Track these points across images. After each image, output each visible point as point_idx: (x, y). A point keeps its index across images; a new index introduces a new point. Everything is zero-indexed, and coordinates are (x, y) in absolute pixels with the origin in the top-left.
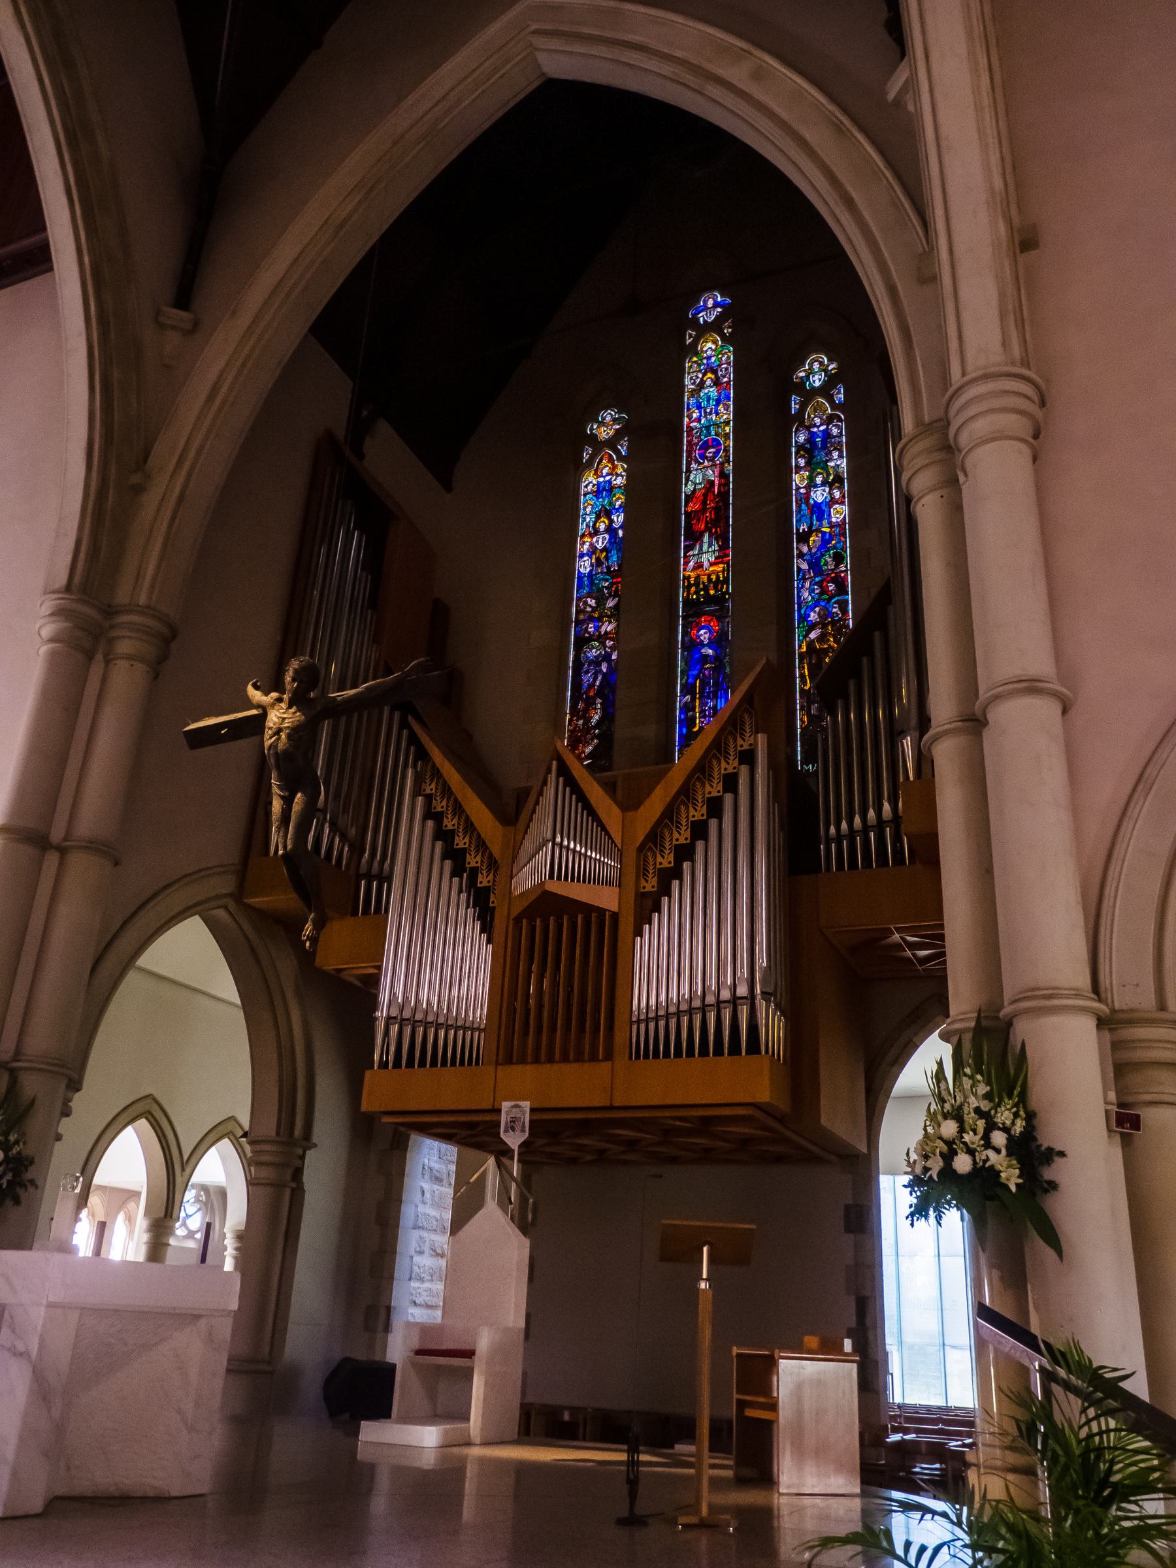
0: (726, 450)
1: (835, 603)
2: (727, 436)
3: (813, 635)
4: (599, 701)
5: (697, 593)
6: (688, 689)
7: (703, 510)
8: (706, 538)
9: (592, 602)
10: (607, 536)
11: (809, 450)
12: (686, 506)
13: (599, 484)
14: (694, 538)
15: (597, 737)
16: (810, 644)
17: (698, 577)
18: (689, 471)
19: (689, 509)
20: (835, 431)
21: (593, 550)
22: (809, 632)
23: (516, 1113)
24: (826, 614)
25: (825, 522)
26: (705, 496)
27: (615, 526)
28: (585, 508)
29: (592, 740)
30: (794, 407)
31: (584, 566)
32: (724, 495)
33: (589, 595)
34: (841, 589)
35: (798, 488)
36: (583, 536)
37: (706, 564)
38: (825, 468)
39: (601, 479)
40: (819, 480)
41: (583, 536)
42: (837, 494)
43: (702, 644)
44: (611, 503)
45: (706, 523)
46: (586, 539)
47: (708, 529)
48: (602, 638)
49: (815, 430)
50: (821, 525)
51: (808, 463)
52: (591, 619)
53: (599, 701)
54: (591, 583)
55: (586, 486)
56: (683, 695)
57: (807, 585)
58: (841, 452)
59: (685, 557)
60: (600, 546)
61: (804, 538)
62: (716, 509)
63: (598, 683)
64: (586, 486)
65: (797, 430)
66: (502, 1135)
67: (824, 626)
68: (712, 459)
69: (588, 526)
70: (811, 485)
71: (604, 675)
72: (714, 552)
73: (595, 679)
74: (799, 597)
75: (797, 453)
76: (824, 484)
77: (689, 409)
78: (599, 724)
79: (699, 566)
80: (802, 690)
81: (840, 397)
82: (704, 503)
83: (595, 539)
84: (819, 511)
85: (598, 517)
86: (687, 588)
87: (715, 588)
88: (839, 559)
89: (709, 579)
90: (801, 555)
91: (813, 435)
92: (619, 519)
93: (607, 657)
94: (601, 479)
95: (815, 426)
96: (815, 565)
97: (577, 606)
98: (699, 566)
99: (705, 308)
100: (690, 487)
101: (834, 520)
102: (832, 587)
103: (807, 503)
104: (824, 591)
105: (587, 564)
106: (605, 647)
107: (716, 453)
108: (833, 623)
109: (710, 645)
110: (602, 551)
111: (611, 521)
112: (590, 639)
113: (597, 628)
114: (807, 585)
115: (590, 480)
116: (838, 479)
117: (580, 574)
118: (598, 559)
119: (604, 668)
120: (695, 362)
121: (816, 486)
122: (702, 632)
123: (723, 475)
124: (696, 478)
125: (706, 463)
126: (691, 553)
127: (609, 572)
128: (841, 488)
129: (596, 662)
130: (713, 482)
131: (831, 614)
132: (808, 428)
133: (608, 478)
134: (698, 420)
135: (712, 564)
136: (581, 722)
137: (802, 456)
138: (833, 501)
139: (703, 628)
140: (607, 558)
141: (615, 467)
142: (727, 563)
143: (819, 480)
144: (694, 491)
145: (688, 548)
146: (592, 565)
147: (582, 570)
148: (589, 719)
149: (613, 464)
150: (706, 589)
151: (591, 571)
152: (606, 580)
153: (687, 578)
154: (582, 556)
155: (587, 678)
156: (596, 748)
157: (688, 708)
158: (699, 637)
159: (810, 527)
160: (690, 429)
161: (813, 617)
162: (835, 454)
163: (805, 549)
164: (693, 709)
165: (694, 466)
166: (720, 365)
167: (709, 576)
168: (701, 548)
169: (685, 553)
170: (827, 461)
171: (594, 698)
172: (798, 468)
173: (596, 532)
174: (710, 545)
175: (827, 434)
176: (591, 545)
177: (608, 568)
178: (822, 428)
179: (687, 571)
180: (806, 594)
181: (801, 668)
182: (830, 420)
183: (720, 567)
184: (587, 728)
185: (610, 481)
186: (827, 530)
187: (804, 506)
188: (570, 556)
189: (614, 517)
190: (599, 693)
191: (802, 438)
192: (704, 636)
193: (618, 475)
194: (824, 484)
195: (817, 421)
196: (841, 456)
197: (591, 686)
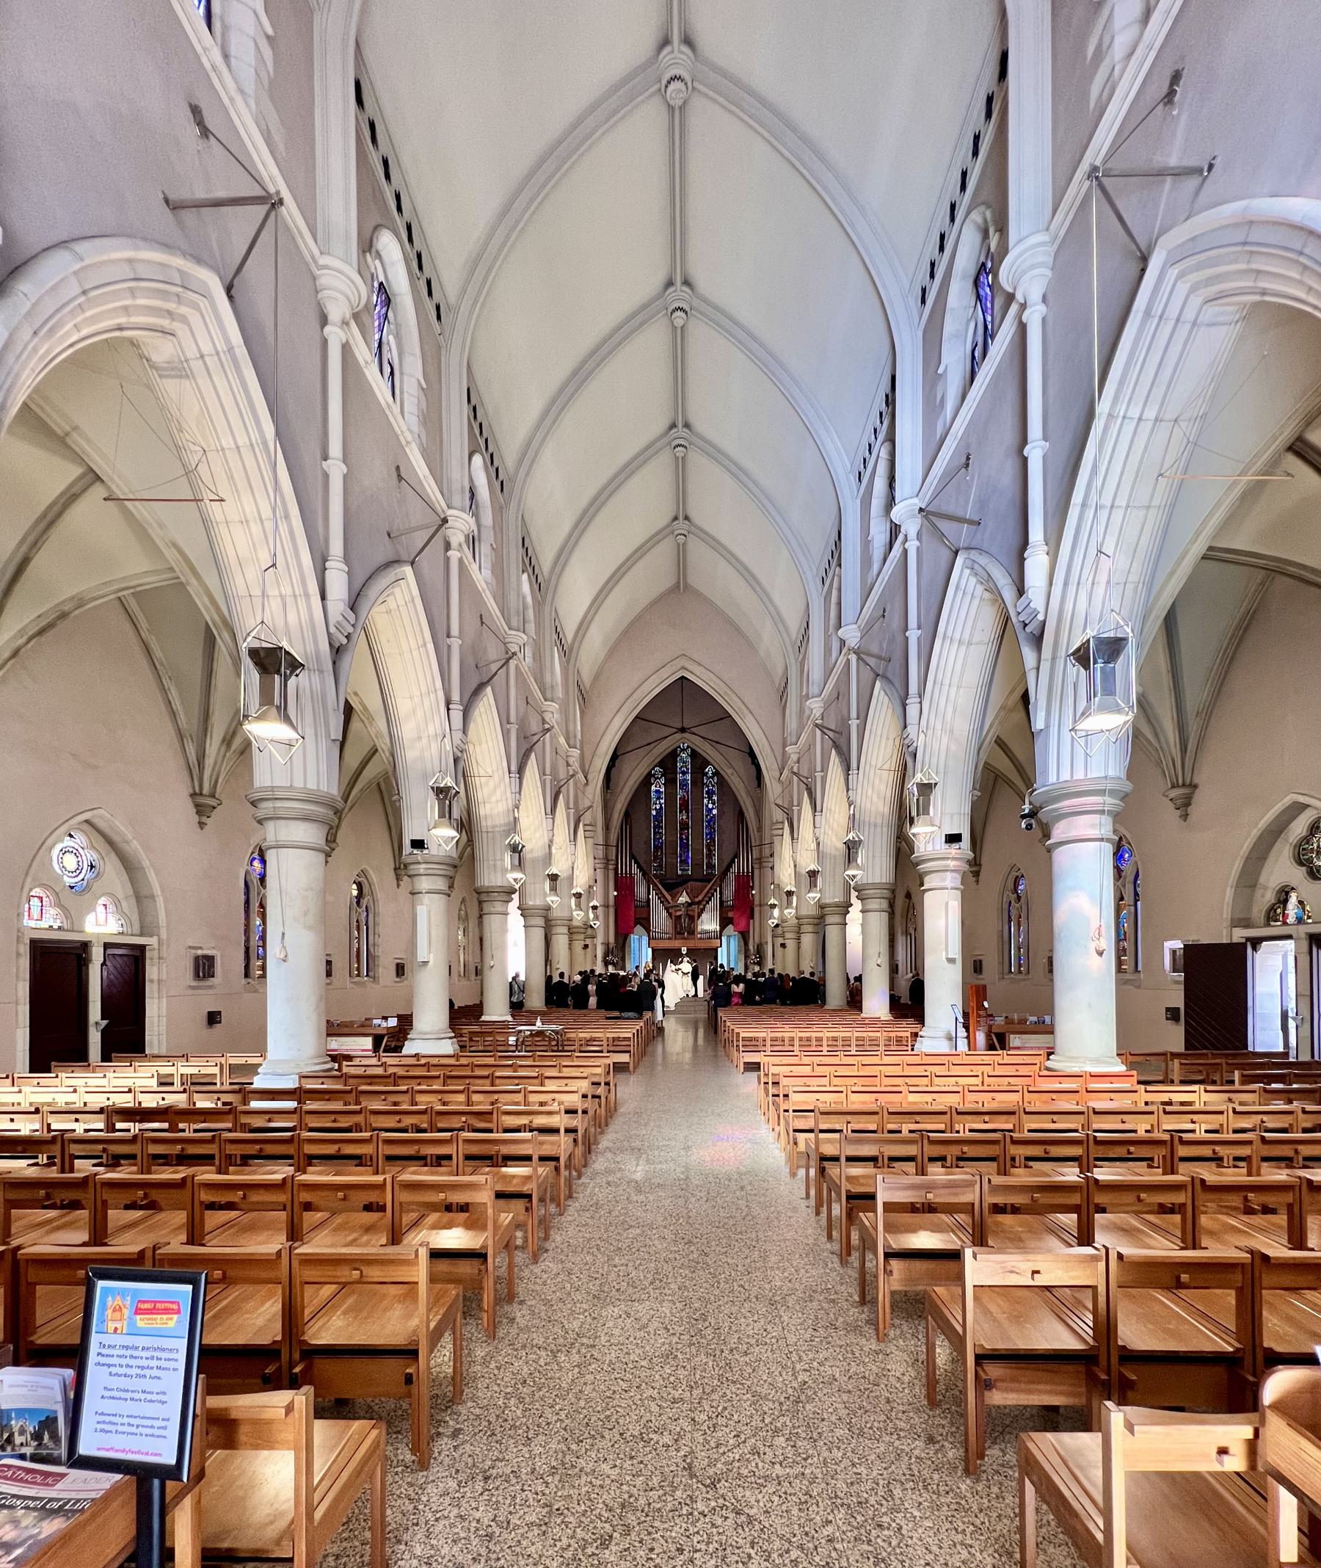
11: (707, 792)
92: (662, 801)
96: (708, 822)
115: (653, 788)
188: (650, 809)
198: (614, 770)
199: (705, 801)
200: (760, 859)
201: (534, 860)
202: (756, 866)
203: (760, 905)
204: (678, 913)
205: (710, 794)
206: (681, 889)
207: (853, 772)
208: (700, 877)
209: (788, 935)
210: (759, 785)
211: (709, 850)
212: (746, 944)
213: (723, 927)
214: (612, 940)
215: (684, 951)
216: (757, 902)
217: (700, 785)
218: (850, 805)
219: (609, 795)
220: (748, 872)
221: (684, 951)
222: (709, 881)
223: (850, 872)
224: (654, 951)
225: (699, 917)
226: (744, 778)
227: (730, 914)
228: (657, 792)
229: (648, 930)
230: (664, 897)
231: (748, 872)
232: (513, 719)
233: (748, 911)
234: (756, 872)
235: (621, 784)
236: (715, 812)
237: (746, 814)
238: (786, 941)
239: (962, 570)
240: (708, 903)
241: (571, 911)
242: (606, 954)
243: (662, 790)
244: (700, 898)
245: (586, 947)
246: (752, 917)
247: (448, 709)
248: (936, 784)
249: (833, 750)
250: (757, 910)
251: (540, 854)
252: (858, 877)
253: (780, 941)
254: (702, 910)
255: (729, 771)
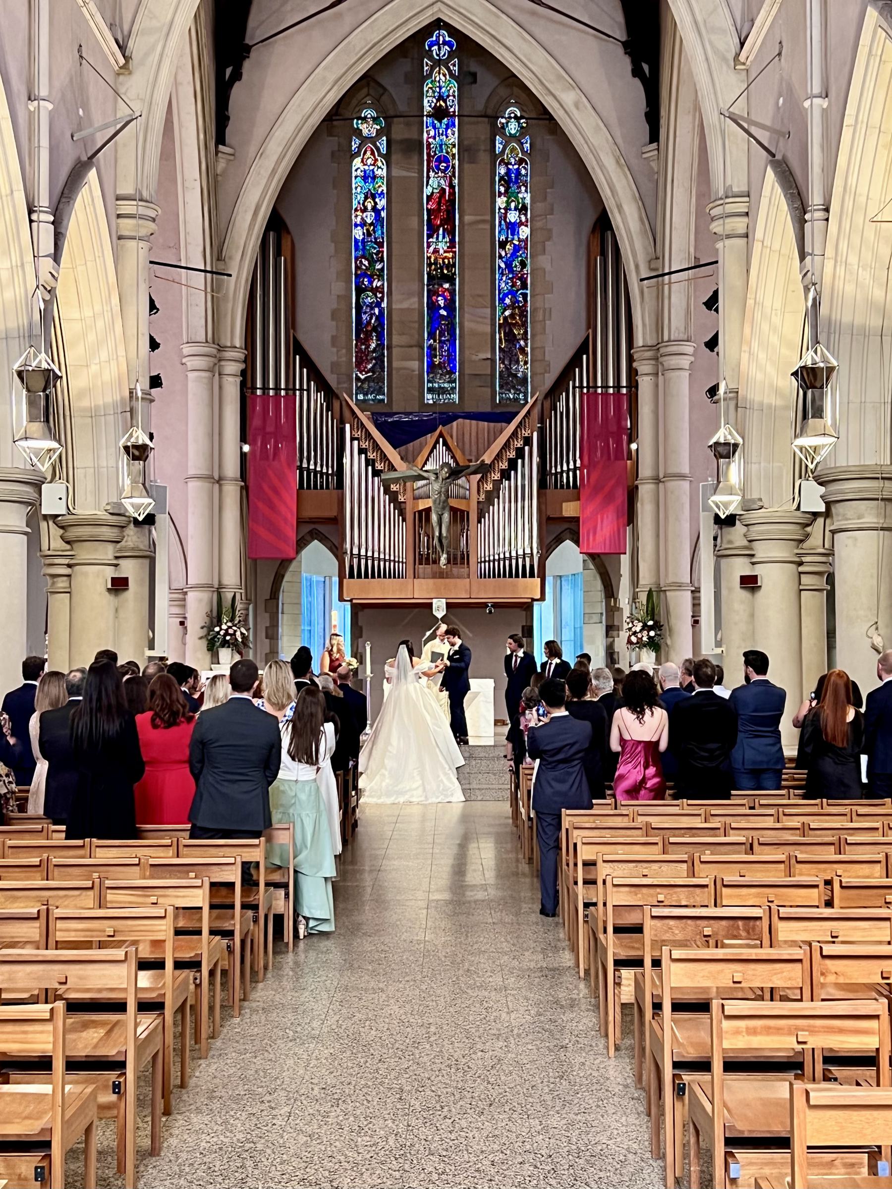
0: (453, 167)
1: (521, 294)
2: (454, 155)
3: (507, 313)
4: (374, 334)
5: (435, 270)
6: (431, 335)
7: (438, 210)
8: (441, 232)
9: (366, 263)
10: (373, 214)
11: (507, 181)
12: (427, 204)
13: (365, 171)
14: (433, 230)
15: (375, 358)
16: (505, 318)
17: (436, 259)
18: (428, 177)
19: (429, 207)
20: (523, 172)
21: (363, 224)
22: (505, 310)
23: (439, 604)
24: (515, 302)
25: (516, 237)
26: (440, 198)
27: (379, 207)
28: (356, 188)
29: (371, 359)
30: (499, 147)
31: (358, 233)
32: (452, 201)
33: (363, 257)
34: (524, 286)
35: (500, 209)
36: (356, 210)
37: (441, 251)
38: (517, 197)
39: (366, 167)
40: (513, 205)
41: (356, 210)
42: (523, 218)
43: (440, 307)
44: (374, 189)
45: (441, 220)
46: (359, 213)
47: (442, 225)
48: (375, 291)
49: (510, 167)
50: (513, 239)
51: (506, 191)
52: (365, 275)
53: (374, 334)
54: (364, 249)
55: (356, 170)
56: (429, 339)
57: (504, 278)
58: (526, 187)
59: (428, 243)
60: (369, 221)
61: (503, 245)
62: (447, 211)
63: (373, 321)
64: (356, 170)
65: (500, 164)
66: (434, 613)
67: (514, 308)
68: (444, 171)
69: (359, 203)
70: (507, 209)
71: (377, 318)
72: (446, 242)
73: (371, 318)
74: (499, 286)
75: (499, 181)
76: (516, 209)
77: (427, 127)
78: (374, 350)
79: (436, 251)
80: (500, 347)
81: (527, 146)
82: (439, 204)
83: (365, 214)
84: (513, 228)
85: (366, 198)
86: (430, 265)
87: (447, 269)
88: (523, 264)
89: (444, 262)
90: (500, 257)
91: (509, 170)
92: (382, 203)
93: (378, 305)
94: (366, 167)
95: (511, 164)
96: (509, 265)
97: (356, 263)
98: (436, 251)
99: (437, 43)
100: (430, 189)
101: (521, 237)
102: (519, 283)
103: (505, 221)
104: (514, 285)
105: (361, 233)
106: (376, 297)
107: (447, 168)
108: (519, 307)
109: (445, 308)
110: (371, 224)
111: (376, 203)
112: (365, 290)
113: (371, 282)
114: (504, 278)
116: (524, 208)
117: (356, 240)
118: (368, 230)
119: (377, 311)
120: (431, 88)
121: (510, 210)
122: (440, 298)
123: (452, 186)
124: (434, 183)
125: (440, 174)
126: (431, 240)
127: (376, 243)
128: (526, 215)
129: (371, 306)
130: (445, 190)
131: (518, 302)
132: (507, 164)
133: (372, 168)
134: (434, 138)
135: (445, 252)
136: (363, 347)
137: (502, 185)
138: (521, 224)
139: (440, 295)
140: (373, 230)
141: (376, 160)
142: (455, 252)
143: (513, 205)
144: (432, 193)
145: (430, 236)
146: (364, 234)
147: (357, 237)
148: (368, 346)
149: (374, 157)
150: (441, 268)
151: (363, 239)
152: (375, 248)
153: (429, 258)
154: (356, 225)
155: (364, 317)
156: (374, 365)
157: (430, 347)
158: (437, 301)
159: (507, 238)
160: (429, 144)
161: (507, 301)
162: (523, 189)
163: (503, 254)
164: (435, 349)
165: (432, 174)
166: (448, 96)
167: (443, 259)
168: (437, 238)
169: (428, 239)
170: (518, 193)
171: (371, 332)
172: (500, 194)
173: (365, 210)
174: (444, 237)
175: (518, 170)
176: (362, 219)
177: (376, 239)
178: (516, 167)
179: (428, 252)
180: (503, 285)
181: (500, 333)
182: (521, 161)
183: (450, 255)
184: (367, 353)
185: (373, 170)
186: (517, 243)
187: (503, 222)
188: (349, 226)
189: (377, 200)
190: (374, 329)
191: (503, 171)
192: (441, 302)
193: (379, 168)
194: (516, 209)
195: (513, 161)
196: (526, 191)
197: (369, 323)
198: (237, 92)
199: (501, 202)
200: (655, 348)
201: (94, 414)
202: (644, 367)
203: (657, 480)
204: (422, 505)
205: (511, 181)
206: (430, 439)
207: (814, 215)
208: (488, 409)
209: (762, 551)
210: (654, 137)
211: (511, 338)
212: (610, 592)
213: (548, 546)
214: (232, 576)
215: (439, 609)
216: (646, 470)
217: (484, 158)
218: (807, 289)
219: (221, 165)
220: (618, 386)
221: (439, 609)
222: (508, 418)
223: (806, 441)
224: (357, 609)
225: (480, 517)
226: (613, 120)
227: (570, 509)
228: (368, 177)
229: (337, 550)
230: (384, 458)
231: (618, 386)
232: (44, 92)
233: (621, 496)
234: (645, 384)
235: (259, 132)
236: (525, 232)
237: (616, 220)
238: (758, 570)
239: (875, 32)
240: (505, 475)
241: (121, 491)
242: (215, 618)
243: (382, 172)
244: (487, 458)
245: (119, 585)
246: (630, 516)
247: (31, 221)
248: (830, 370)
249: (769, 169)
250: (645, 491)
251: (109, 400)
252: (824, 452)
253: (740, 567)
254: (491, 497)
255: (569, 98)
